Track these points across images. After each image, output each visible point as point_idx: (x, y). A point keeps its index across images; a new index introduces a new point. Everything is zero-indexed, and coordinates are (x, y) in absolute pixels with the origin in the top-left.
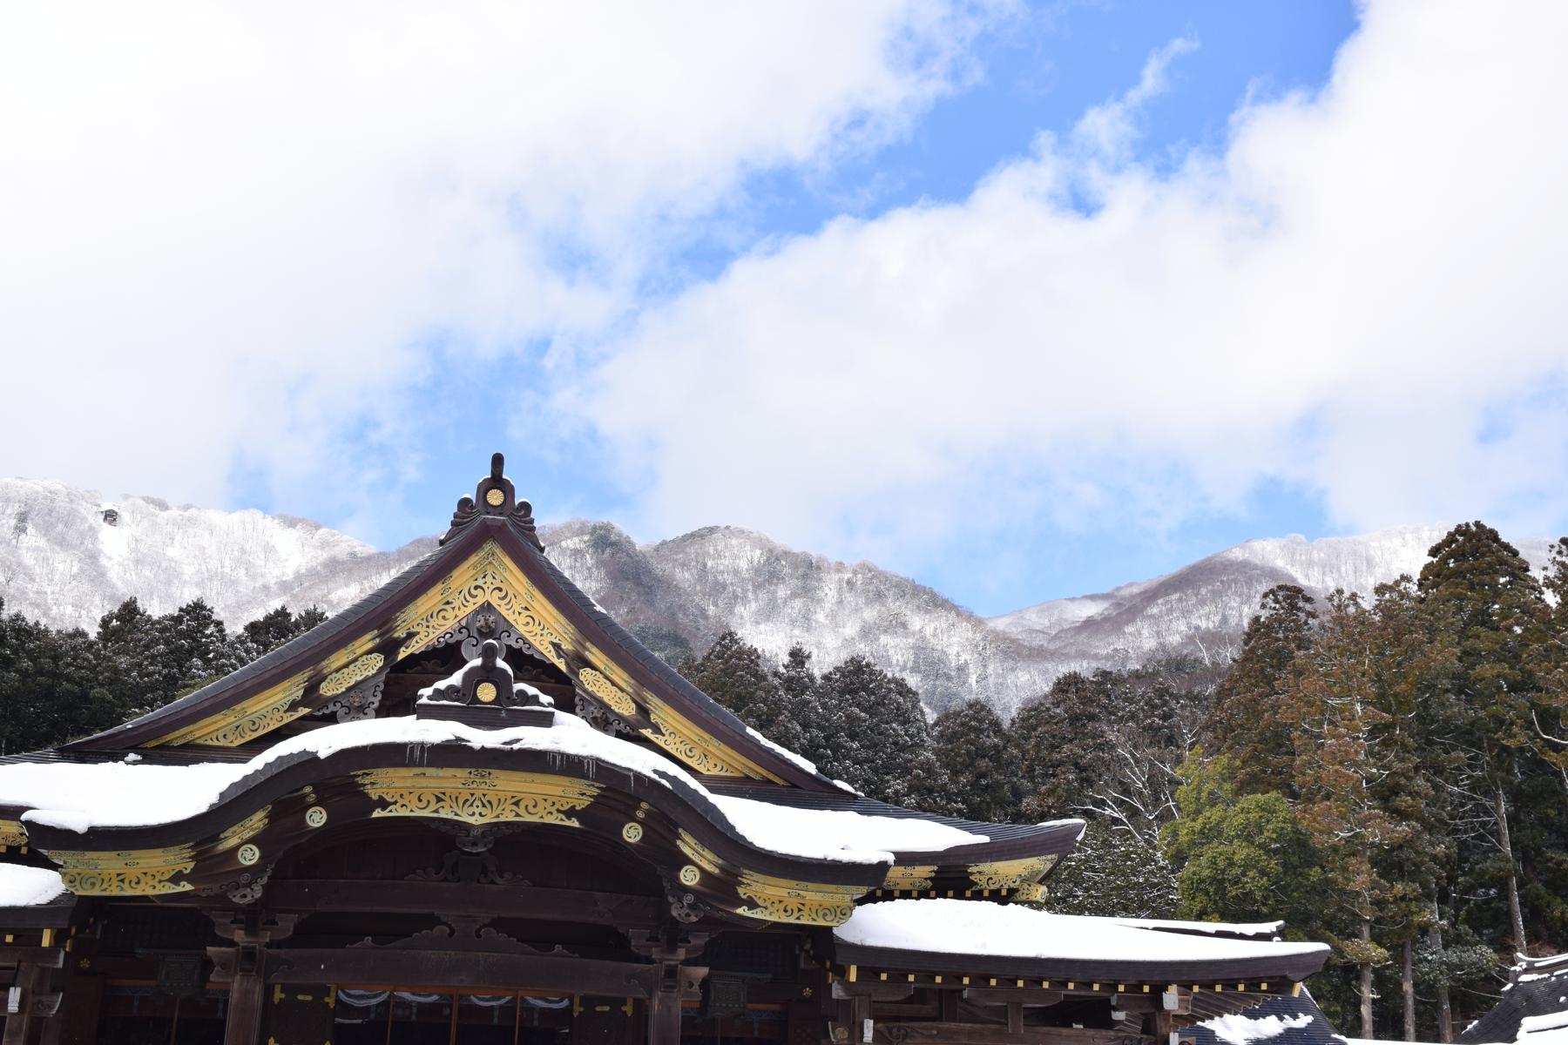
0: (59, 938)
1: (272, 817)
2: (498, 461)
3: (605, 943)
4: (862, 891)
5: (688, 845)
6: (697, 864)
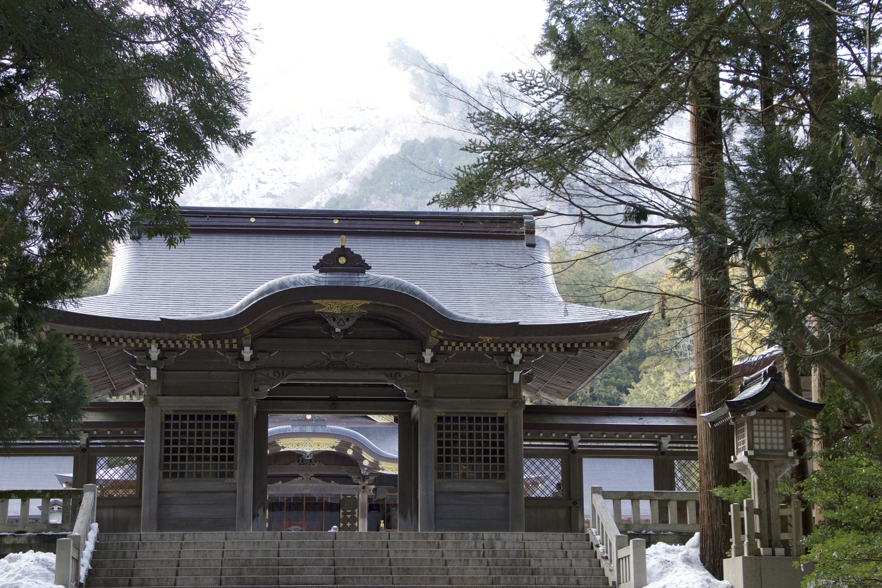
5: (364, 455)
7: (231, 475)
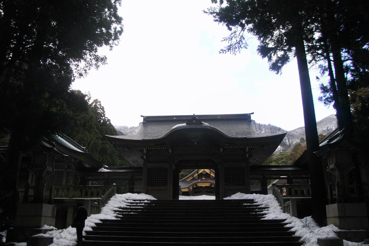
7: (166, 185)
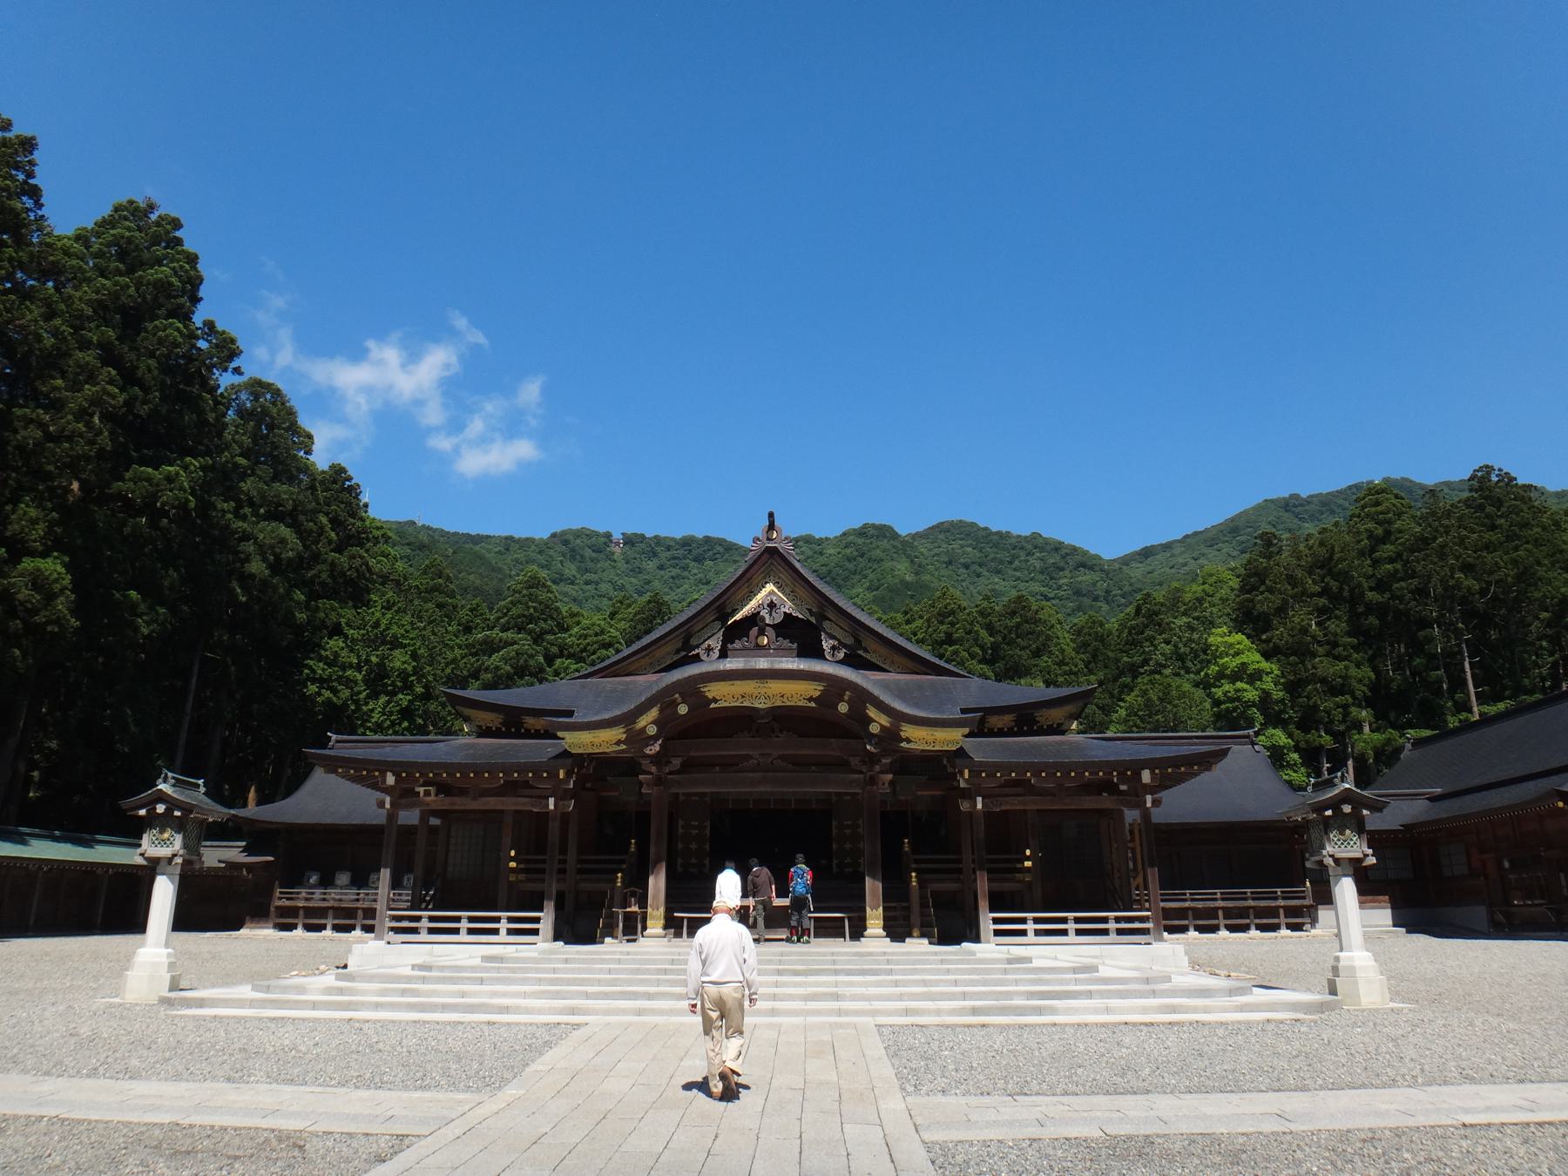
0: (569, 774)
1: (661, 711)
2: (771, 515)
3: (842, 765)
4: (966, 731)
5: (872, 712)
6: (879, 721)
